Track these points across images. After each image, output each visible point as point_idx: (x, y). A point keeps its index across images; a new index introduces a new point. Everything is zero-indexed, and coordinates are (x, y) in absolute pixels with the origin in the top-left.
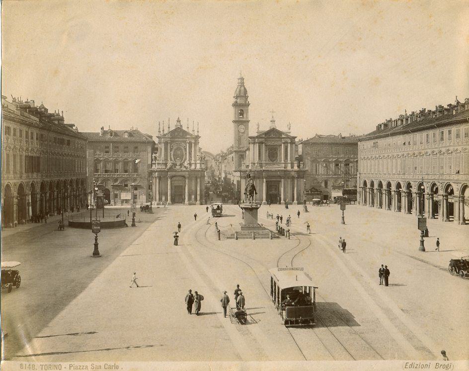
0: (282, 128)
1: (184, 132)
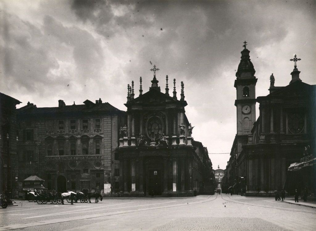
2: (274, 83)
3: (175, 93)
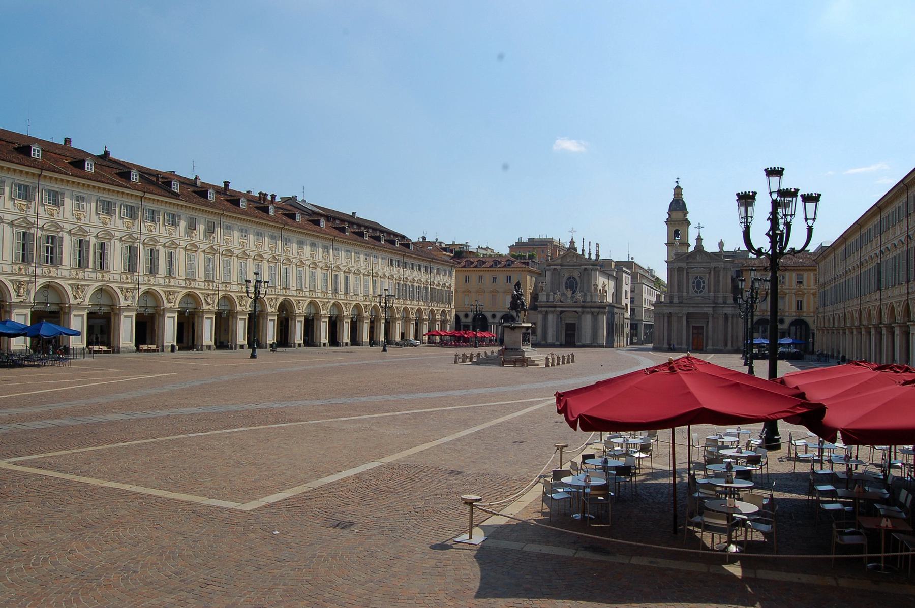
1: (578, 255)
3: (590, 254)
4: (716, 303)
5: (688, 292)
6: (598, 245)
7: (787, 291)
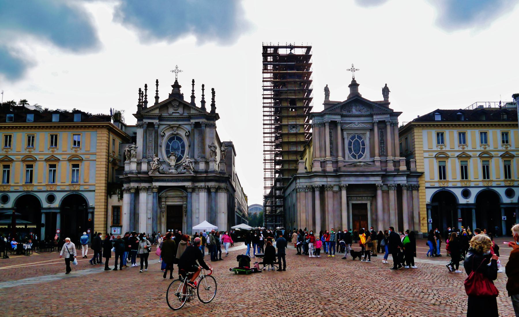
0: (371, 94)
1: (186, 106)
2: (329, 95)
3: (203, 102)
4: (386, 170)
5: (344, 157)
6: (213, 89)
7: (471, 154)
